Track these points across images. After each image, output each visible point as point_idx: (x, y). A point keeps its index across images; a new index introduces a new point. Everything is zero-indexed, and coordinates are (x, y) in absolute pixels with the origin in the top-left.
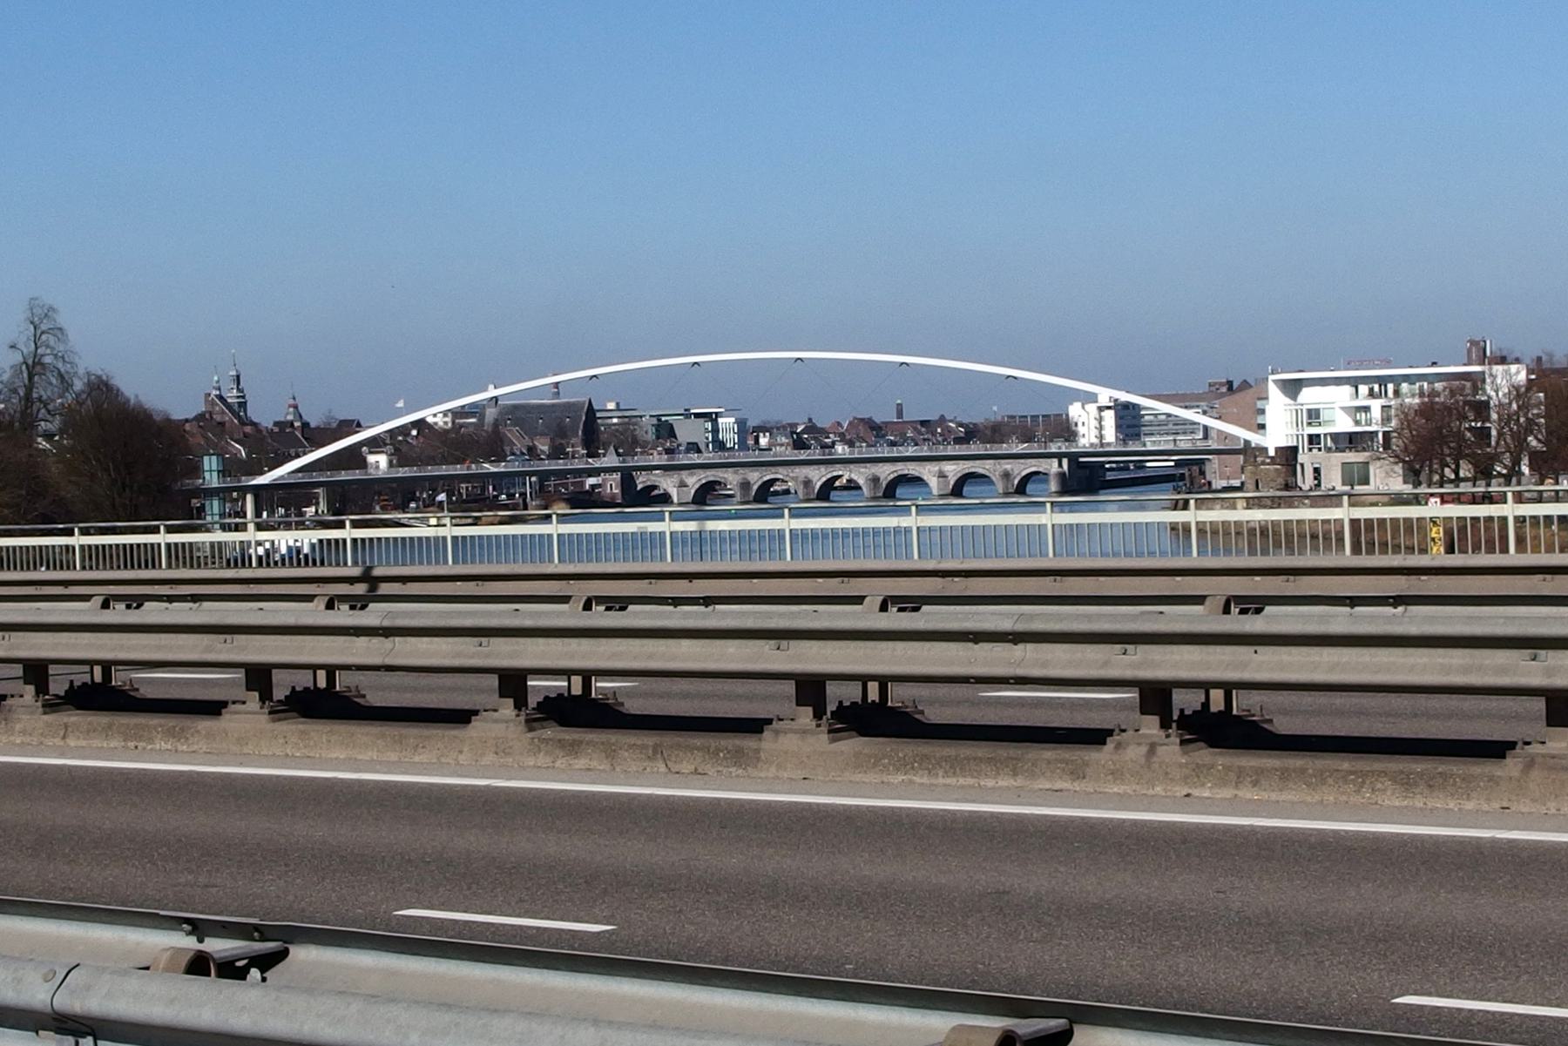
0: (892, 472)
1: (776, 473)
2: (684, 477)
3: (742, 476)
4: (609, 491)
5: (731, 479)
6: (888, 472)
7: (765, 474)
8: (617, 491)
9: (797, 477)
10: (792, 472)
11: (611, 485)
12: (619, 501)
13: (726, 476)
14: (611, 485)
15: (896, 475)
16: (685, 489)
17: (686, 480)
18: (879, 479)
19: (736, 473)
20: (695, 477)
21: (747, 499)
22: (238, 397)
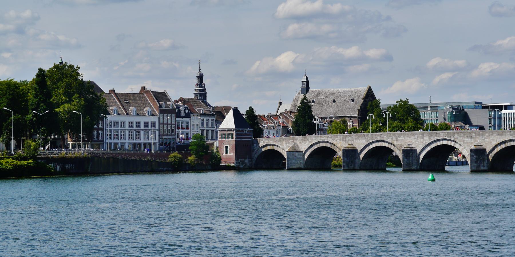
0: (500, 144)
1: (381, 141)
2: (298, 142)
3: (350, 143)
4: (225, 154)
5: (339, 145)
6: (495, 143)
7: (371, 141)
8: (232, 154)
9: (401, 146)
10: (397, 140)
11: (227, 147)
12: (232, 165)
13: (334, 142)
14: (227, 147)
15: (503, 146)
17: (299, 145)
18: (485, 150)
19: (343, 139)
20: (308, 142)
21: (352, 167)
22: (200, 90)
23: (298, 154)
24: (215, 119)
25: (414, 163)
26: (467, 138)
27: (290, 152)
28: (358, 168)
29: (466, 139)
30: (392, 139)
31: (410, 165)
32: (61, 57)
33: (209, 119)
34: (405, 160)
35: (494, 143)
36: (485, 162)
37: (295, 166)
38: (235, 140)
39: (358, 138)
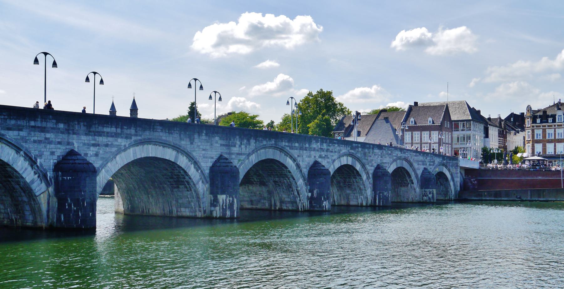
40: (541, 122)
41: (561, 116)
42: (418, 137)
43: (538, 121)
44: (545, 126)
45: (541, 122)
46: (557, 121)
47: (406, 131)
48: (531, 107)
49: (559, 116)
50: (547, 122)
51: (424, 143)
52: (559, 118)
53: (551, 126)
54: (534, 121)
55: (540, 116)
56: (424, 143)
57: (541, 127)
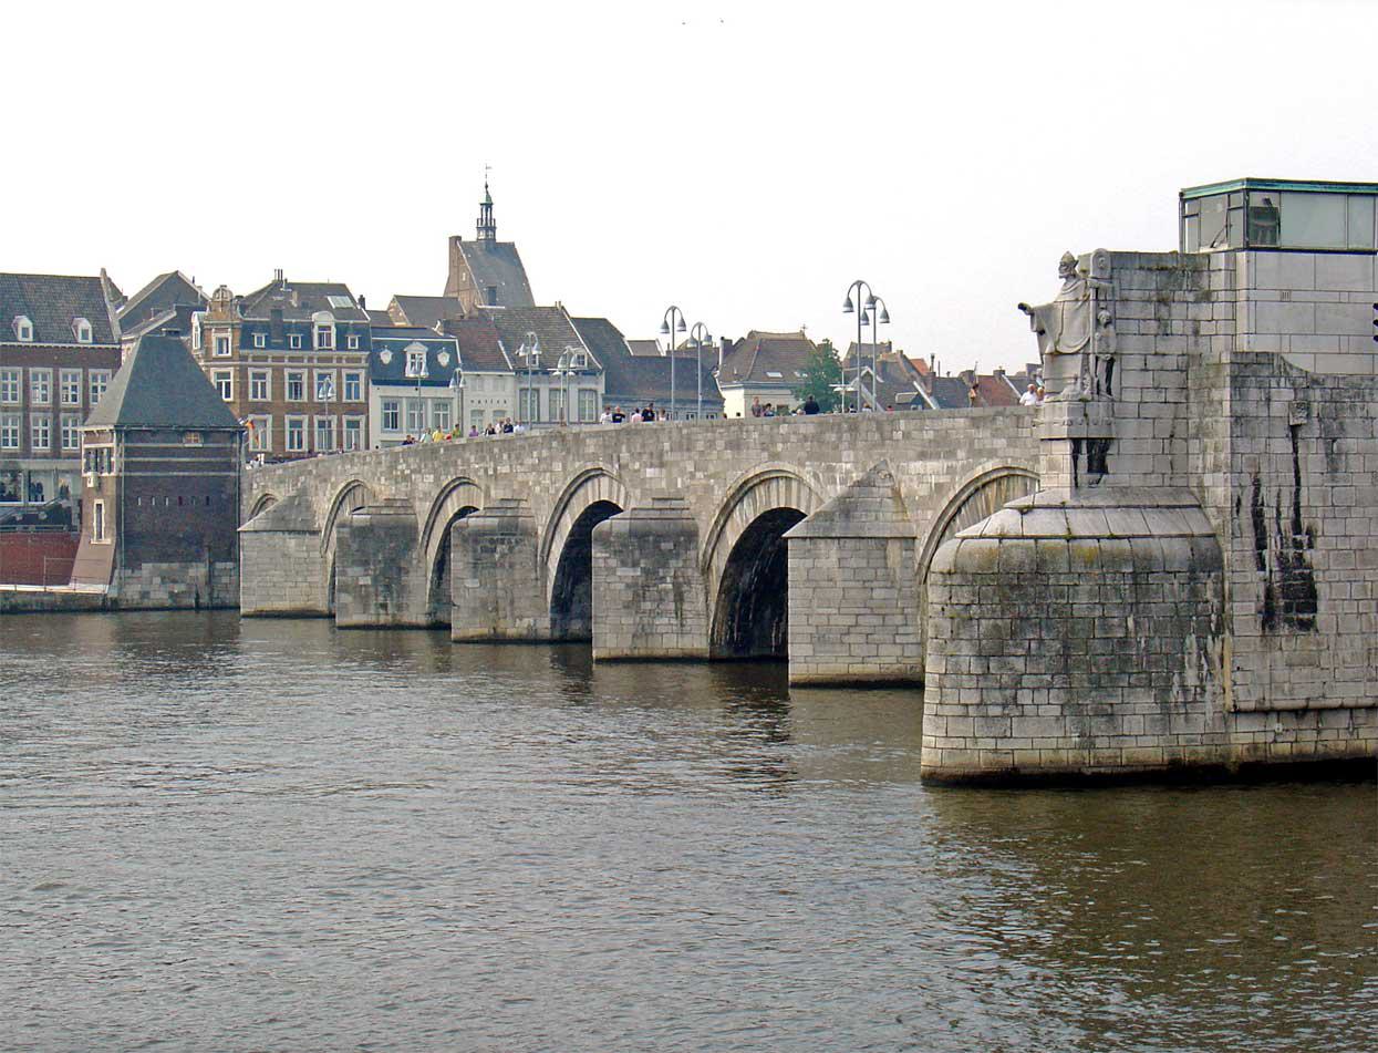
16: (291, 542)
18: (691, 535)
23: (298, 545)
24: (601, 389)
25: (522, 603)
26: (651, 466)
27: (256, 532)
28: (422, 620)
29: (650, 472)
30: (486, 470)
31: (496, 609)
32: (487, 187)
33: (538, 390)
34: (470, 583)
35: (720, 495)
36: (686, 606)
37: (281, 598)
38: (118, 477)
39: (418, 471)
40: (269, 346)
41: (329, 328)
42: (14, 387)
43: (259, 339)
44: (281, 359)
45: (269, 346)
46: (316, 344)
47: (422, 385)
48: (231, 293)
49: (321, 328)
50: (286, 346)
51: (66, 410)
52: (320, 336)
53: (300, 359)
54: (246, 342)
55: (265, 327)
56: (15, 409)
57: (270, 362)
